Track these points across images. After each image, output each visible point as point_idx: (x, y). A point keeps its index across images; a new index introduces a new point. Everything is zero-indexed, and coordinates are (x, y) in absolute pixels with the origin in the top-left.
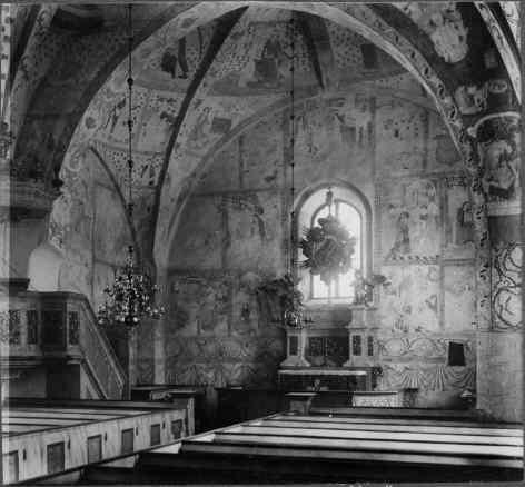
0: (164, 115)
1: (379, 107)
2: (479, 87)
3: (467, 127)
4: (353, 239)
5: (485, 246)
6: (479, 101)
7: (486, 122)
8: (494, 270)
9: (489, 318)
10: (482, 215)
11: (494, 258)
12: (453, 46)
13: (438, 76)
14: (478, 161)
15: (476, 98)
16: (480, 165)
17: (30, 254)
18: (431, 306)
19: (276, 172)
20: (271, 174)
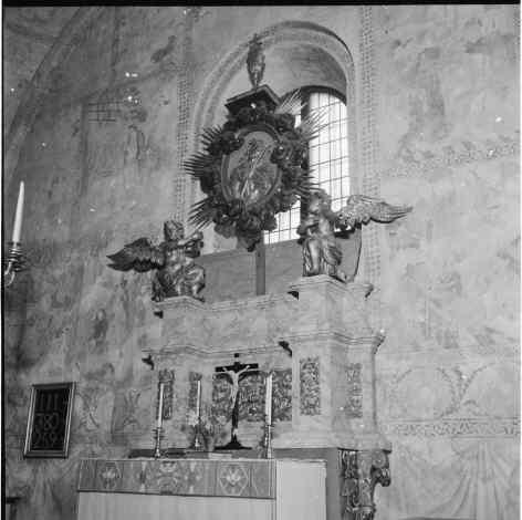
19: (172, 39)
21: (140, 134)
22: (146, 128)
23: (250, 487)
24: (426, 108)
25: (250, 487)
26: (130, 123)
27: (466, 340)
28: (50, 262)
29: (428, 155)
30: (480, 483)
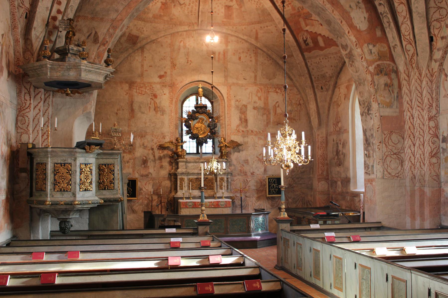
1: (229, 42)
2: (374, 46)
3: (369, 66)
5: (379, 132)
6: (374, 53)
7: (378, 65)
8: (384, 145)
9: (382, 171)
10: (377, 114)
11: (384, 139)
12: (362, 22)
13: (354, 36)
14: (375, 85)
15: (373, 51)
16: (376, 87)
17: (74, 121)
20: (162, 73)
21: (155, 103)
22: (157, 101)
23: (226, 205)
24: (243, 120)
25: (226, 205)
26: (151, 97)
27: (249, 174)
29: (243, 131)
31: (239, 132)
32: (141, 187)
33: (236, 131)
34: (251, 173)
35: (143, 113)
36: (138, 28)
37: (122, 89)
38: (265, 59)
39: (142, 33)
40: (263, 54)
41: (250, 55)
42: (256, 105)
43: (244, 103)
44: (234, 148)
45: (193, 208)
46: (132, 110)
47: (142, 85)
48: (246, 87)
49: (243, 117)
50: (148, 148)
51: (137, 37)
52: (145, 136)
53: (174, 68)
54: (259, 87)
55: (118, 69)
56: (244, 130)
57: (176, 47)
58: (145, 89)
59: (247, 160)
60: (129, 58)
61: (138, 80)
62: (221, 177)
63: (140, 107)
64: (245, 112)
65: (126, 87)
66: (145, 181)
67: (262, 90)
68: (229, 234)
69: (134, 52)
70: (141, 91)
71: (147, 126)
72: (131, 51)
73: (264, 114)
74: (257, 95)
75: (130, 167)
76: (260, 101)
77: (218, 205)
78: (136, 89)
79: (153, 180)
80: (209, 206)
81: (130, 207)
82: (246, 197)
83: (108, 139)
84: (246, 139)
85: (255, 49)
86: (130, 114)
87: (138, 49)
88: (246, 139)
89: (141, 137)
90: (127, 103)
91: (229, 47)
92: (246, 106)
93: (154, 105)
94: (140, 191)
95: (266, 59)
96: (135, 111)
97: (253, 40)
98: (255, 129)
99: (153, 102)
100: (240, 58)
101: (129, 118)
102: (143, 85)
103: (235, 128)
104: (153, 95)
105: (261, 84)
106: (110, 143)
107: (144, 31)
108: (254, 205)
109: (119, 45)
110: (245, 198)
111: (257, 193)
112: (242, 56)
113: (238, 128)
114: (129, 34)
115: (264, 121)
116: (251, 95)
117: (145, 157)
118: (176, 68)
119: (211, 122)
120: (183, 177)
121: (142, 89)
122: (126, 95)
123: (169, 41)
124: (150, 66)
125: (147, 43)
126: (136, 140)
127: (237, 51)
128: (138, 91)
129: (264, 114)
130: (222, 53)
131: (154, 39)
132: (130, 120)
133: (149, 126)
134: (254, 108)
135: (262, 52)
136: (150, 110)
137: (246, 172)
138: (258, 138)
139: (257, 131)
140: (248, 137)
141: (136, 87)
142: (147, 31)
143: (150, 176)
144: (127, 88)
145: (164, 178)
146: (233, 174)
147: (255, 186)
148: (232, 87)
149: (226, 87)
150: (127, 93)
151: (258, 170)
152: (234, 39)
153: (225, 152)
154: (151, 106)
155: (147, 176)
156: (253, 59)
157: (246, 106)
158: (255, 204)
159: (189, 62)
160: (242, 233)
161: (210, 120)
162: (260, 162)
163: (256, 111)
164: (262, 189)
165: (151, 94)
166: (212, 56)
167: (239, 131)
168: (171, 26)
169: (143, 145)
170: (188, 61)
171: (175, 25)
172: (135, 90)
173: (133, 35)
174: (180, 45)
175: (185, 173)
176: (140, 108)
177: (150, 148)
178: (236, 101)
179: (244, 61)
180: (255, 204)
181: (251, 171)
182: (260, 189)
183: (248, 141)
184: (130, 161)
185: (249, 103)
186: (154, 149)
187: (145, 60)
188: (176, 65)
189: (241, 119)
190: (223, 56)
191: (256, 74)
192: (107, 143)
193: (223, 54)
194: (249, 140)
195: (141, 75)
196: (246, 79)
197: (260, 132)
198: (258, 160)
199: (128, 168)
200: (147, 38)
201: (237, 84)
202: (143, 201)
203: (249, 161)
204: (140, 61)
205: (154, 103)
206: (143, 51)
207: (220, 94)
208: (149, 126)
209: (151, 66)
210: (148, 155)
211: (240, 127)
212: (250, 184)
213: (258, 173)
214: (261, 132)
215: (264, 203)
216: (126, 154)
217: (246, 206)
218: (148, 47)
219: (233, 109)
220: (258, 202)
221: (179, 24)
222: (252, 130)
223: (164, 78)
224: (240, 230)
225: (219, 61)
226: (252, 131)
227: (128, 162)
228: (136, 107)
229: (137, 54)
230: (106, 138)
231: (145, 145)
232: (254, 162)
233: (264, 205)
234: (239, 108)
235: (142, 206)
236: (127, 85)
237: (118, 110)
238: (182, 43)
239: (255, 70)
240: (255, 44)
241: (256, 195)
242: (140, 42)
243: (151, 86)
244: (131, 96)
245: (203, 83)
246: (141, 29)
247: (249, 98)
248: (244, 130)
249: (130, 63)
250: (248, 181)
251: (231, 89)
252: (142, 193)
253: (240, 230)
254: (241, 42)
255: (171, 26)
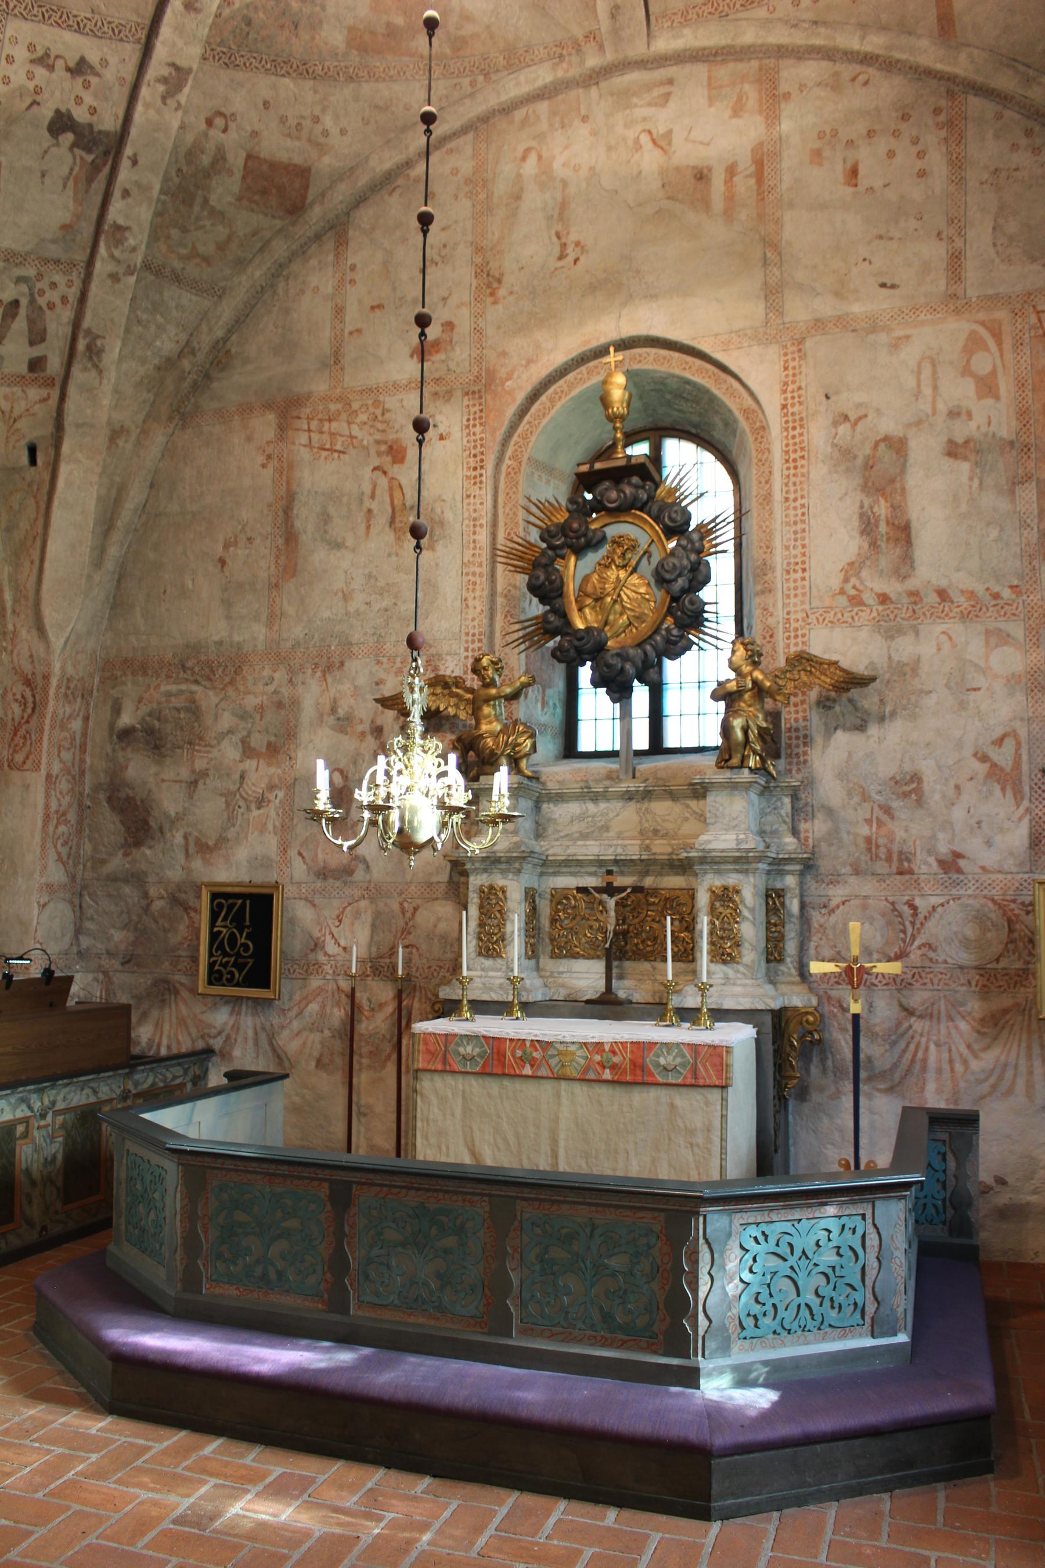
0: (61, 123)
1: (787, 96)
4: (706, 531)
18: (995, 772)
24: (883, 528)
26: (376, 462)
27: (925, 866)
28: (232, 682)
29: (884, 599)
30: (932, 1048)
31: (861, 603)
32: (316, 934)
33: (843, 601)
34: (941, 863)
35: (338, 545)
36: (292, 122)
37: (249, 439)
38: (1014, 147)
39: (322, 149)
40: (999, 116)
41: (915, 141)
42: (961, 431)
43: (888, 426)
44: (824, 704)
45: (483, 1073)
46: (291, 537)
47: (333, 407)
48: (899, 333)
49: (882, 509)
50: (360, 728)
51: (303, 173)
52: (342, 664)
53: (492, 294)
54: (981, 316)
55: (233, 350)
56: (893, 588)
57: (500, 189)
58: (349, 423)
59: (916, 778)
60: (281, 286)
61: (320, 386)
62: (718, 882)
63: (325, 518)
64: (892, 481)
65: (265, 425)
66: (336, 903)
67: (997, 336)
68: (517, 1341)
69: (301, 253)
70: (332, 435)
71: (351, 609)
72: (280, 249)
73: (1016, 482)
74: (966, 371)
75: (270, 827)
76: (990, 401)
77: (638, 1066)
78: (309, 430)
79: (372, 900)
80: (586, 1069)
81: (263, 1037)
82: (910, 1012)
83: (181, 692)
84: (905, 648)
85: (943, 103)
86: (278, 557)
87: (318, 237)
88: (905, 648)
89: (324, 672)
90: (270, 506)
91: (786, 126)
92: (898, 446)
93: (387, 499)
94: (311, 956)
95: (1023, 142)
96: (303, 538)
97: (924, 43)
98: (962, 581)
99: (383, 482)
100: (853, 174)
101: (274, 581)
102: (339, 406)
103: (836, 583)
104: (384, 448)
105: (992, 301)
106: (188, 710)
107: (326, 133)
108: (959, 1067)
109: (208, 223)
110: (899, 1024)
111: (984, 993)
112: (868, 157)
113: (853, 581)
114: (249, 157)
115: (1024, 525)
116: (926, 373)
117: (341, 772)
118: (502, 292)
119: (673, 553)
120: (499, 881)
121: (334, 425)
122: (264, 466)
123: (466, 167)
124: (373, 308)
125: (360, 201)
126: (300, 689)
127: (835, 133)
128: (315, 437)
129: (1016, 482)
130: (746, 164)
131: (388, 165)
132: (277, 585)
133: (363, 608)
134: (953, 450)
135: (989, 108)
136: (368, 527)
137: (905, 857)
138: (988, 632)
139: (979, 589)
140: (917, 633)
141: (309, 419)
142: (343, 132)
143: (359, 874)
144: (271, 434)
145: (429, 885)
146: (824, 865)
147: (966, 943)
148: (809, 344)
149: (773, 352)
150: (269, 457)
151: (989, 843)
152: (811, 70)
153: (745, 730)
154: (374, 506)
155: (345, 872)
156: (937, 161)
157: (898, 446)
158: (965, 1062)
159: (570, 250)
160: (622, 1345)
161: (672, 544)
162: (997, 789)
163: (965, 467)
164: (1019, 965)
165: (378, 442)
166: (430, 13)
167: (856, 601)
168: (466, 82)
169: (334, 710)
170: (564, 246)
171: (486, 75)
172: (303, 438)
173: (274, 166)
174: (519, 176)
175: (510, 860)
176: (326, 523)
177: (366, 727)
178: (835, 424)
179: (878, 183)
180: (965, 1062)
181: (943, 849)
182: (1002, 964)
183: (918, 661)
184: (272, 797)
185: (919, 423)
186: (386, 729)
187: (352, 282)
188: (499, 281)
189: (868, 526)
190: (752, 181)
191: (959, 243)
192: (178, 710)
193: (753, 169)
194: (926, 649)
195: (335, 360)
196: (893, 286)
197: (996, 596)
198: (989, 775)
199: (262, 832)
200: (352, 169)
201: (843, 323)
202: (323, 1007)
203: (926, 787)
204: (330, 290)
205: (391, 489)
206: (342, 242)
207: (749, 402)
208: (363, 608)
209: (380, 306)
210: (355, 763)
211: (864, 574)
212: (933, 929)
213: (989, 858)
214: (1006, 594)
215: (1029, 1057)
216: (254, 762)
217: (908, 1071)
218: (365, 216)
219: (818, 472)
220: (987, 1048)
221: (501, 61)
222: (943, 583)
223: (441, 356)
224: (607, 1318)
225: (729, 214)
226: (943, 594)
227: (261, 802)
228: (305, 518)
229: (313, 262)
230: (173, 688)
231: (341, 712)
232: (957, 787)
233: (1031, 1073)
234: (860, 461)
235: (316, 1038)
236: (271, 417)
237: (226, 546)
238: (532, 159)
239: (951, 221)
240: (939, 66)
241: (975, 1006)
242: (323, 195)
243: (377, 403)
244: (286, 470)
245: (653, 351)
246: (307, 124)
247: (917, 394)
248: (893, 588)
249: (287, 311)
250: (923, 911)
251: (803, 357)
252: (319, 965)
253: (607, 1318)
254: (853, 80)
255: (466, 82)
